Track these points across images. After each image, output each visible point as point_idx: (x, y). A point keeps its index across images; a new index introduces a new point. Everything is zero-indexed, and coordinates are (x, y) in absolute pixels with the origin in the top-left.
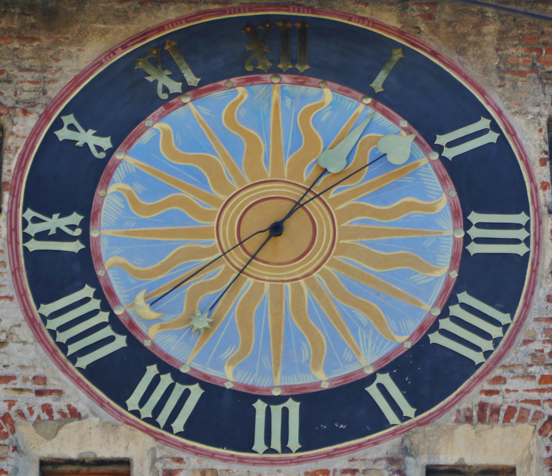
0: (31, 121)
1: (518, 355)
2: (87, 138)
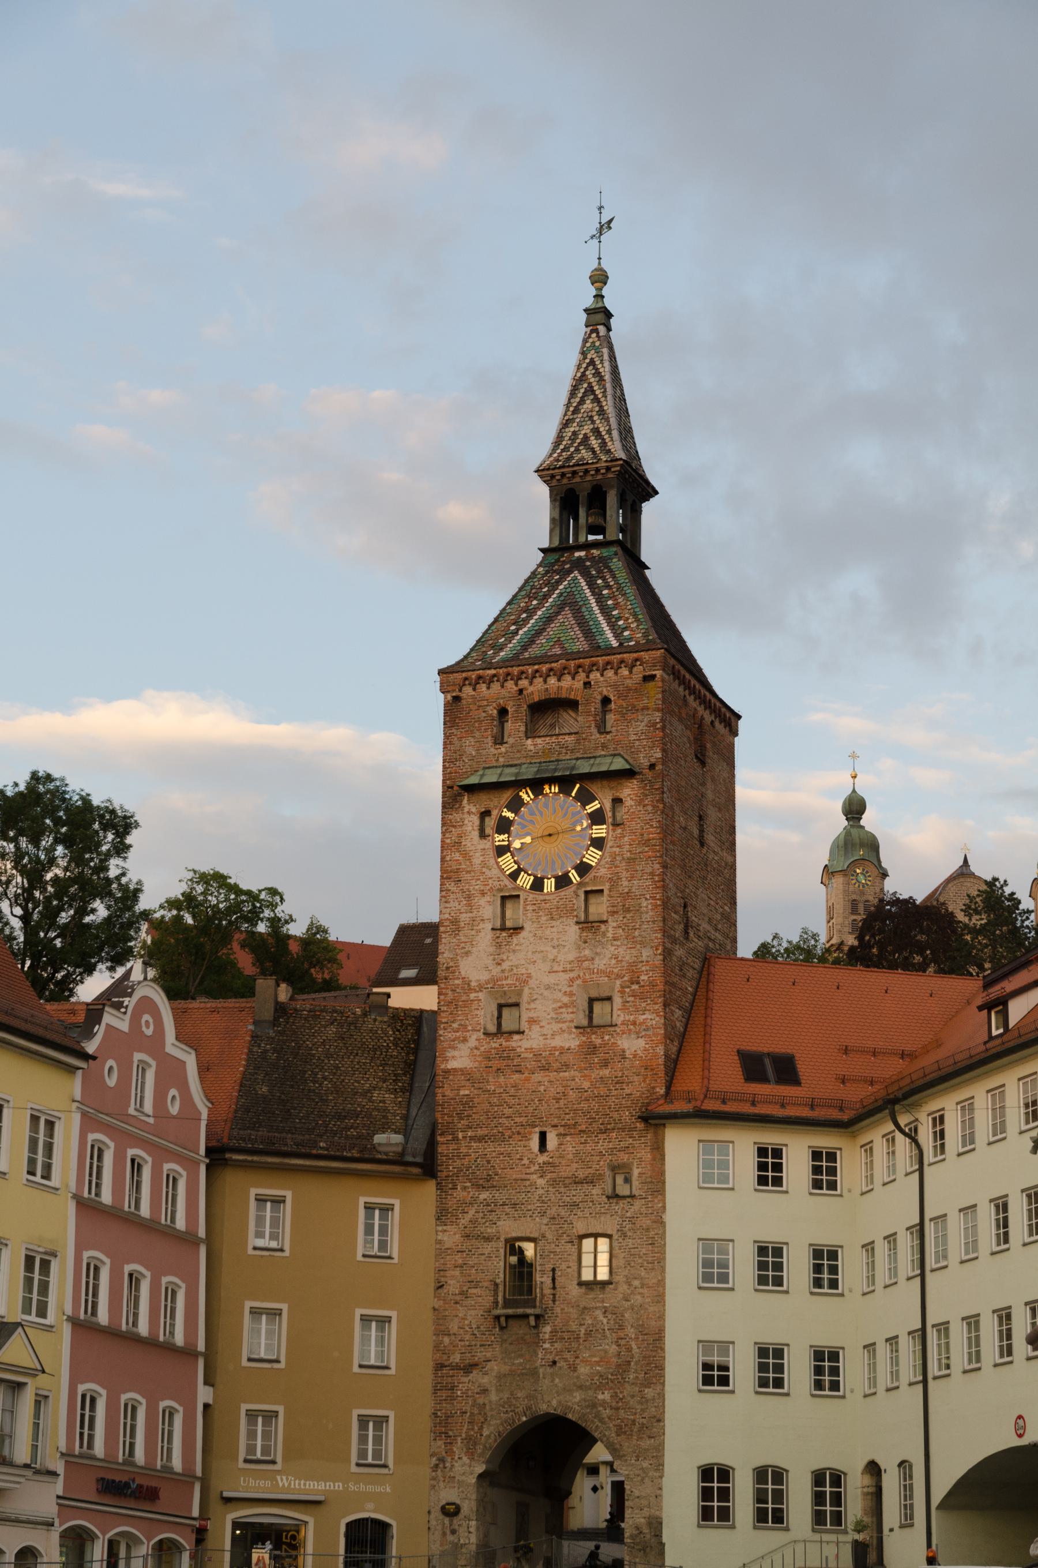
1: (603, 862)
2: (510, 815)
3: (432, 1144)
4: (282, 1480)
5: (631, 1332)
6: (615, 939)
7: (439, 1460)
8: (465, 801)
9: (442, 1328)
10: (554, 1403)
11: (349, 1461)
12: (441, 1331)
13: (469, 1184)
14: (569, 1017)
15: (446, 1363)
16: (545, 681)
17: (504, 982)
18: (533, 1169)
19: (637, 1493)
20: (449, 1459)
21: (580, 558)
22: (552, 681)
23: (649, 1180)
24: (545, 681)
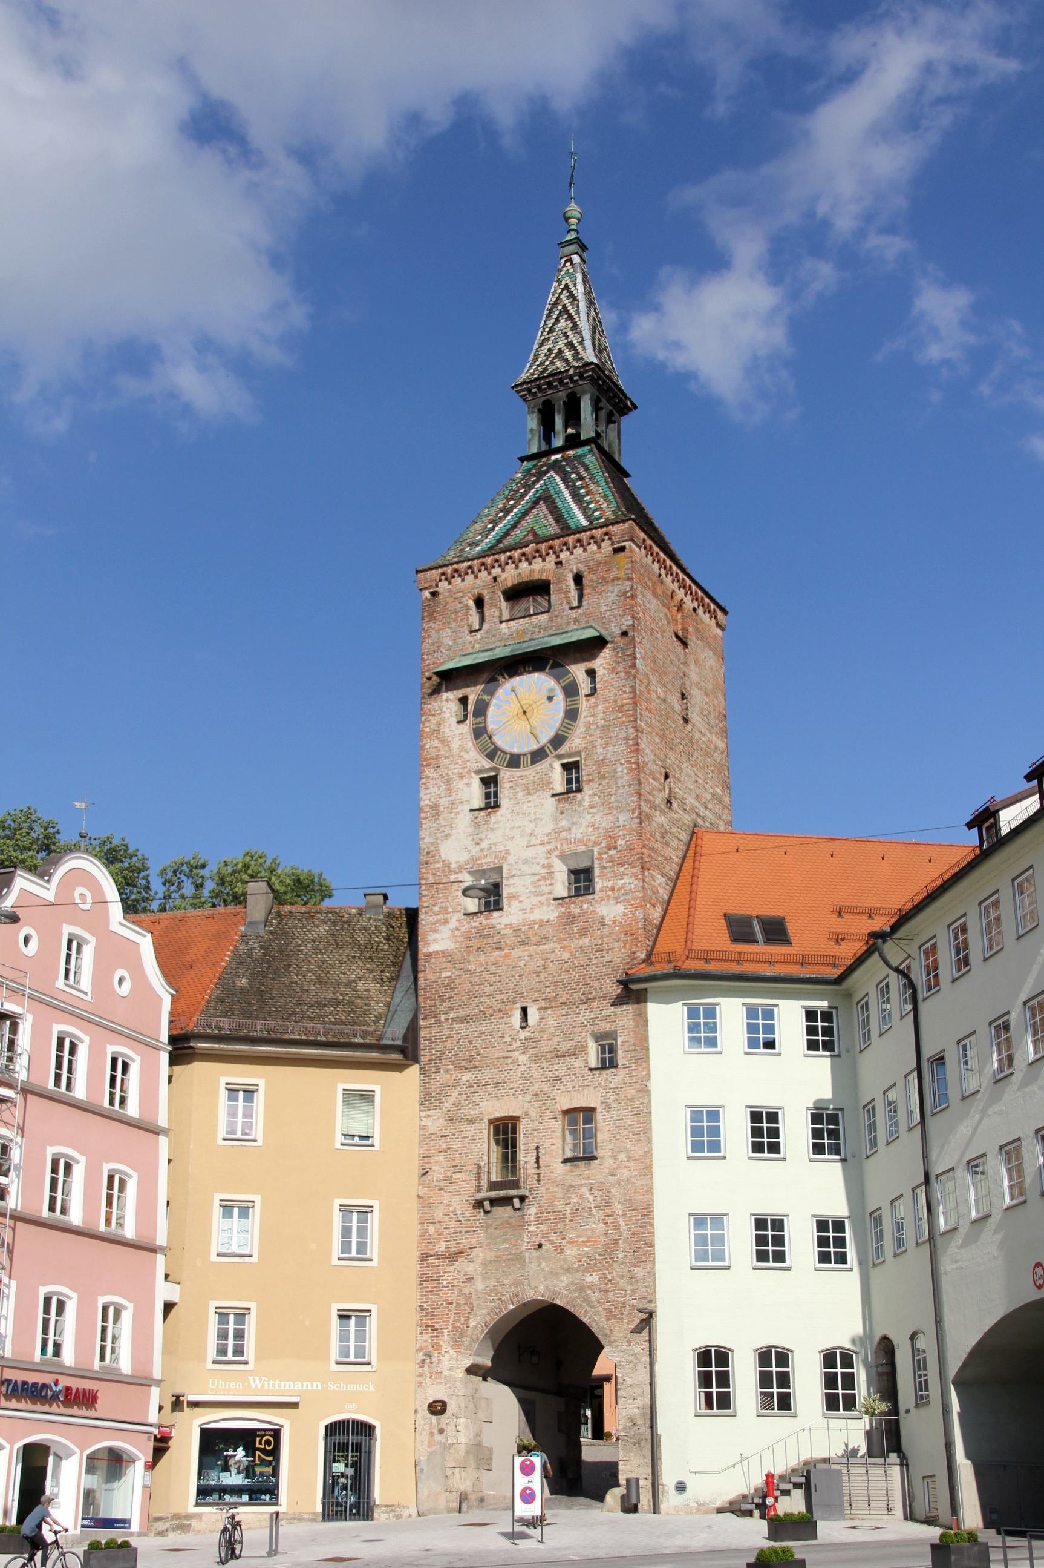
3: (413, 1029)
4: (254, 1380)
5: (618, 1208)
6: (591, 807)
7: (426, 1355)
9: (427, 1216)
10: (541, 1288)
11: (327, 1357)
12: (427, 1220)
13: (451, 1067)
14: (546, 889)
15: (432, 1253)
16: (517, 567)
17: (484, 861)
18: (514, 1047)
19: (629, 1381)
20: (436, 1353)
21: (556, 461)
22: (524, 565)
23: (632, 1048)
24: (517, 567)
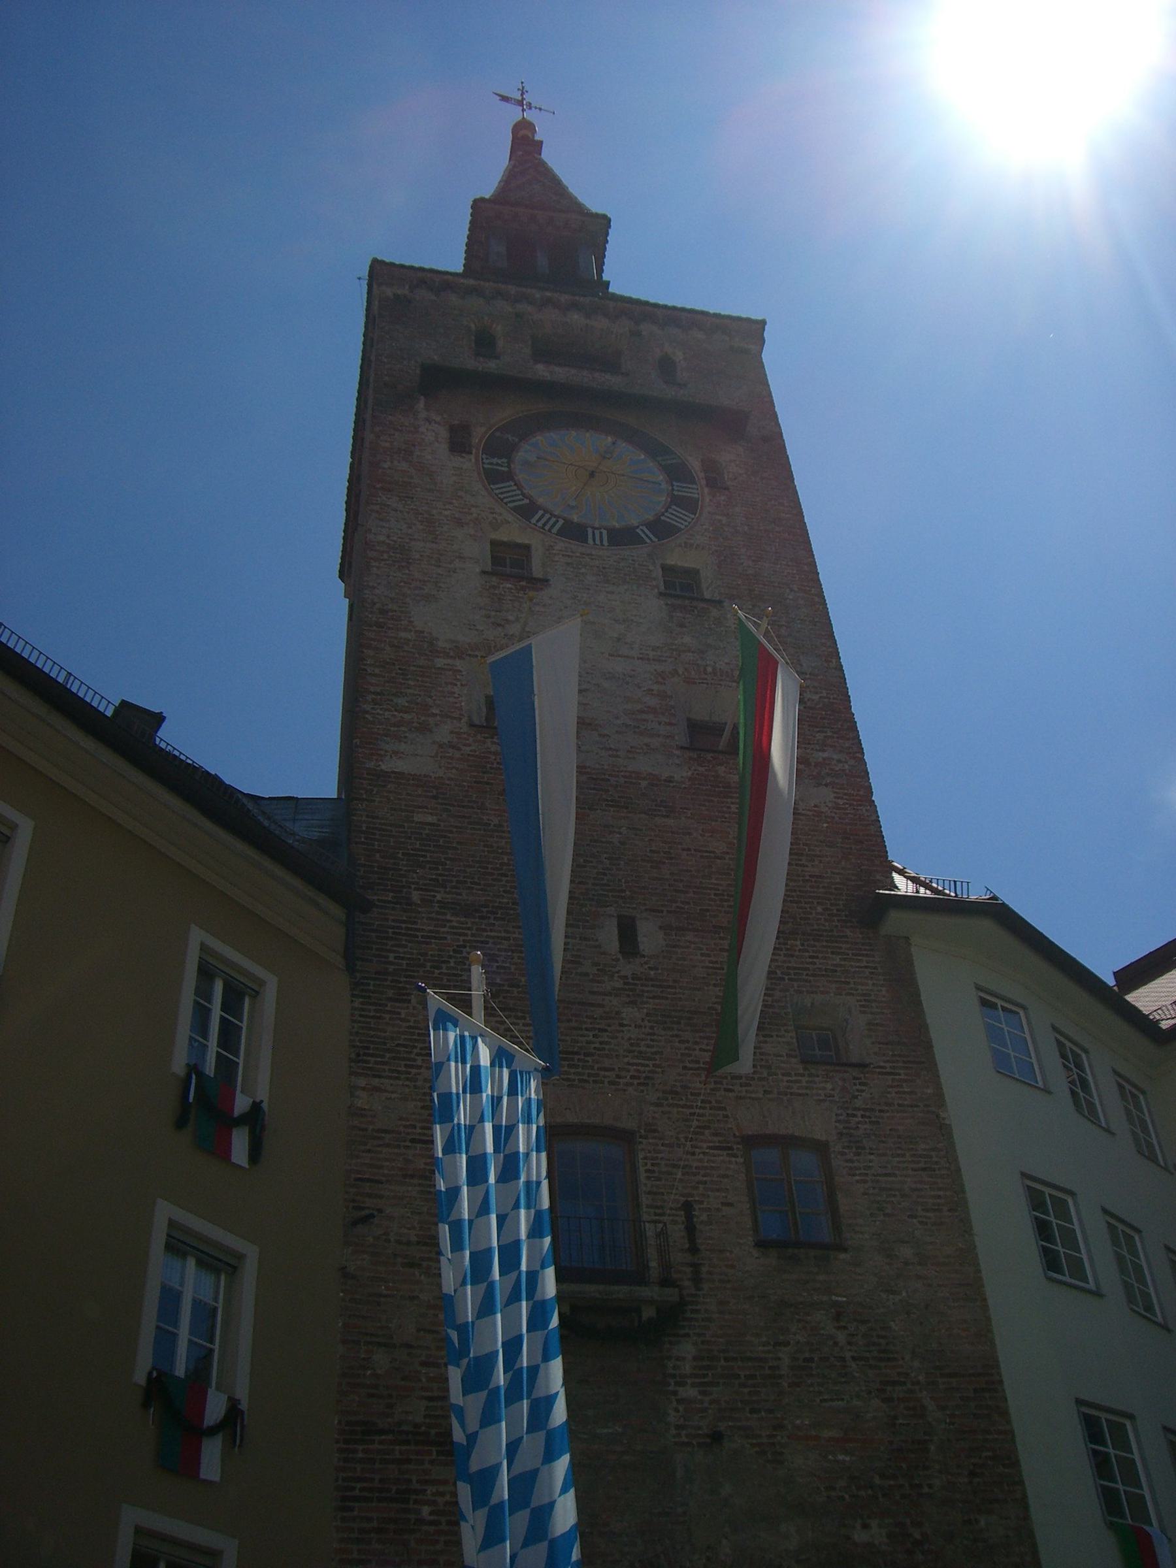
0: (483, 429)
8: (421, 405)
